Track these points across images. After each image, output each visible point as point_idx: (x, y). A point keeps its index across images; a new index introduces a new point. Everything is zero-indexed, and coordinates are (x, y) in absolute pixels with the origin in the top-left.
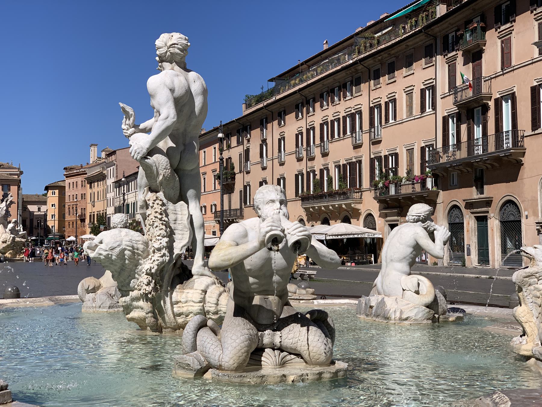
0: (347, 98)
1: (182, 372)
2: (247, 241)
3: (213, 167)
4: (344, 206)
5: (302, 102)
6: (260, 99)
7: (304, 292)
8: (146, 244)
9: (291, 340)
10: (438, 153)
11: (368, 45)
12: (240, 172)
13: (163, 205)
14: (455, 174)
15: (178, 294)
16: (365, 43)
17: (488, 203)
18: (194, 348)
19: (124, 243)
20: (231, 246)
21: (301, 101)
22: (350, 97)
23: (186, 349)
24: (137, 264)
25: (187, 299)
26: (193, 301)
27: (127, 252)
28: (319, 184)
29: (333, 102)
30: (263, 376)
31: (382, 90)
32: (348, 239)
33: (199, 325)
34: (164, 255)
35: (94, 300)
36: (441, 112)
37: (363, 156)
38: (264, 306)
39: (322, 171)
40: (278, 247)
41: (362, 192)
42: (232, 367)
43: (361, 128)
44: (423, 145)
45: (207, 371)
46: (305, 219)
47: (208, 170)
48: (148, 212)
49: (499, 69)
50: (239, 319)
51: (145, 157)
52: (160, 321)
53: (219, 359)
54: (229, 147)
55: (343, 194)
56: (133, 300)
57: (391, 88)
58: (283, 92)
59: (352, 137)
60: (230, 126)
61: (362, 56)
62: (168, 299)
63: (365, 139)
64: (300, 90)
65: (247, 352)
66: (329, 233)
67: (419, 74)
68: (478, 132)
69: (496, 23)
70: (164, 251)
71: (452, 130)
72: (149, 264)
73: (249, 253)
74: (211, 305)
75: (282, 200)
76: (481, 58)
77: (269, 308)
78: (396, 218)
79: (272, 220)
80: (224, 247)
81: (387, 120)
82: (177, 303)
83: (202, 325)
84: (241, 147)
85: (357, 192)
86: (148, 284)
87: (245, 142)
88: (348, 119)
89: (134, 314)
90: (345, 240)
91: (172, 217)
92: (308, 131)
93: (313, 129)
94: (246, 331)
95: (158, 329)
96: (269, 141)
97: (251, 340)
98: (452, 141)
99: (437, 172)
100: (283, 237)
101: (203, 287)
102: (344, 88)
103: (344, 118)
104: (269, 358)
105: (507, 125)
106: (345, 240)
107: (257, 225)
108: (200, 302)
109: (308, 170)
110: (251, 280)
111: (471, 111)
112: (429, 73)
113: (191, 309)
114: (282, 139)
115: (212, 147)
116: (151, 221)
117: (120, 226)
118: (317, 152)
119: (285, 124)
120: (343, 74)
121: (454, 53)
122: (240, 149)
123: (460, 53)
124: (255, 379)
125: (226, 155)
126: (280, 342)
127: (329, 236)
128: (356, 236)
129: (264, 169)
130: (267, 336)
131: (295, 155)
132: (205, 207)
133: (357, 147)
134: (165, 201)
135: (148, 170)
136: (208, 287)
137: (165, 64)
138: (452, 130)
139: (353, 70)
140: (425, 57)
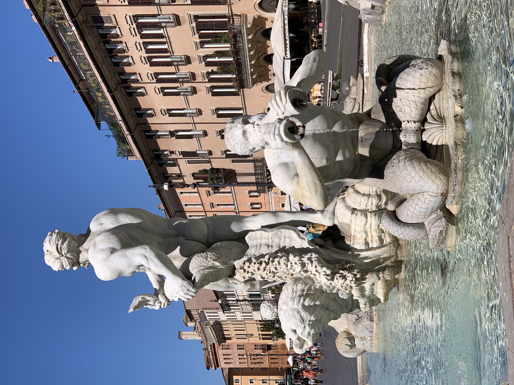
0: (119, 33)
1: (450, 240)
2: (293, 163)
3: (204, 195)
4: (250, 37)
5: (125, 88)
7: (354, 89)
8: (297, 280)
9: (413, 109)
11: (52, 7)
12: (210, 162)
13: (249, 260)
15: (356, 242)
16: (50, 11)
18: (420, 226)
19: (295, 306)
20: (298, 183)
21: (123, 90)
22: (118, 29)
23: (422, 235)
24: (321, 291)
25: (362, 232)
26: (365, 225)
27: (306, 303)
28: (224, 67)
30: (456, 144)
32: (290, 32)
33: (393, 221)
34: (310, 259)
35: (363, 339)
37: (189, 13)
38: (371, 142)
39: (208, 64)
40: (300, 126)
41: (232, 15)
42: (444, 181)
43: (154, 16)
45: (448, 210)
46: (266, 84)
47: (208, 201)
48: (258, 278)
50: (387, 172)
51: (193, 283)
52: (388, 263)
53: (435, 197)
54: (180, 176)
55: (235, 38)
56: (363, 295)
58: (113, 112)
59: (166, 27)
60: (155, 174)
61: (67, 14)
62: (363, 254)
64: (109, 90)
65: (426, 163)
70: (305, 260)
72: (320, 276)
73: (307, 162)
74: (370, 203)
75: (242, 121)
77: (373, 136)
79: (267, 134)
80: (300, 191)
82: (367, 243)
83: (394, 216)
84: (179, 161)
85: (233, 21)
86: (344, 277)
87: (173, 156)
88: (144, 32)
89: (380, 293)
90: (291, 35)
91: (264, 250)
92: (159, 81)
93: (156, 74)
94: (401, 164)
95: (397, 266)
96: (173, 128)
97: (411, 158)
100: (288, 120)
101: (349, 213)
102: (106, 38)
103: (143, 36)
104: (434, 136)
106: (291, 35)
107: (274, 151)
108: (366, 216)
109: (207, 80)
110: (339, 158)
113: (374, 227)
114: (170, 112)
115: (180, 196)
116: (269, 275)
117: (275, 310)
118: (185, 70)
119: (151, 109)
120: (88, 38)
122: (183, 162)
124: (459, 154)
125: (189, 180)
126: (414, 122)
127: (286, 54)
128: (286, 22)
129: (205, 134)
130: (407, 138)
131: (189, 97)
132: (252, 204)
133: (177, 21)
134: (245, 258)
135: (206, 279)
136: (348, 207)
137: (82, 259)
139: (84, 26)
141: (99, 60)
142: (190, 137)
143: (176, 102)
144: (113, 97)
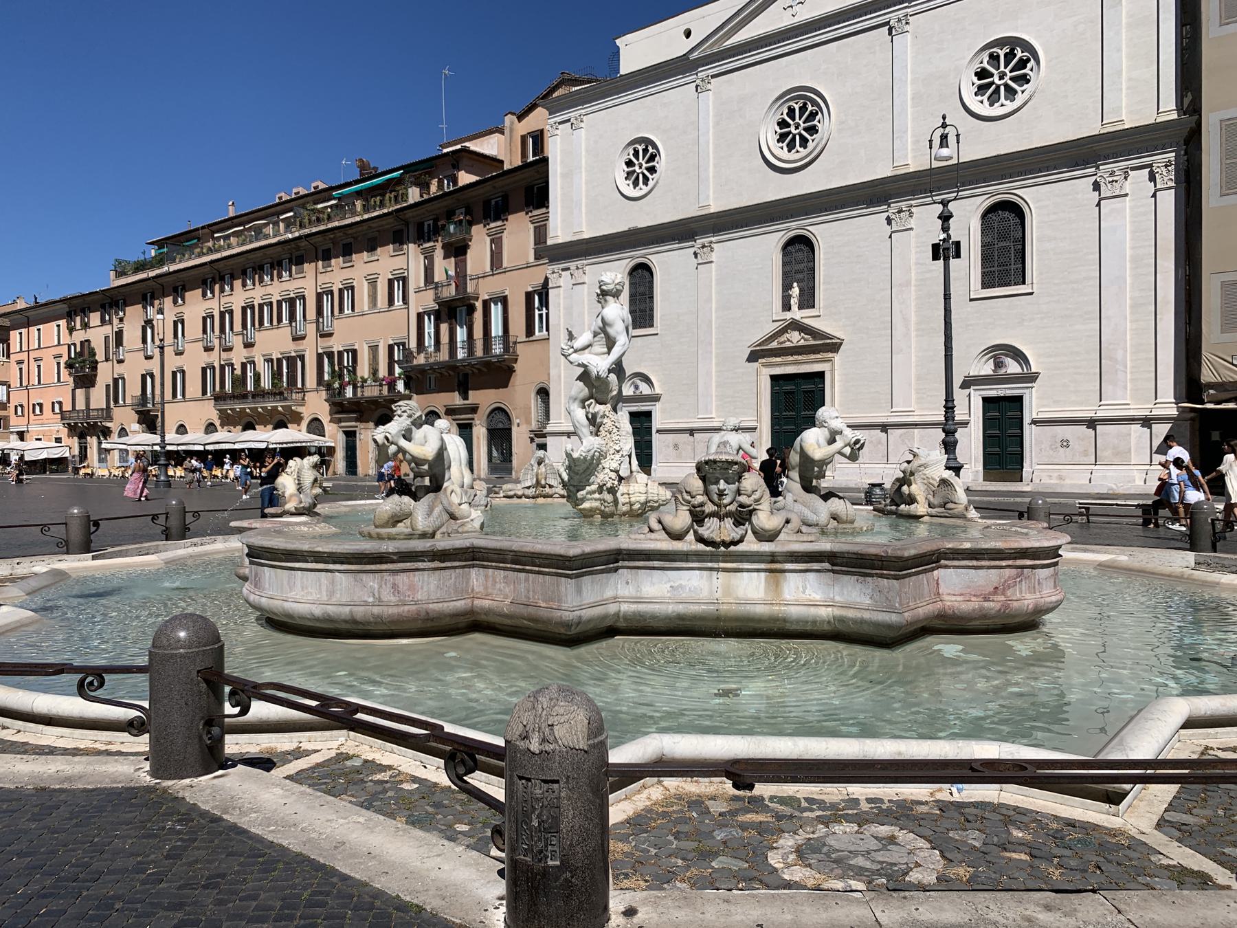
5: (214, 277)
6: (140, 267)
10: (412, 353)
11: (314, 218)
12: (107, 360)
14: (433, 377)
17: (474, 409)
28: (240, 381)
29: (261, 280)
31: (336, 274)
36: (414, 309)
39: (244, 366)
44: (391, 342)
46: (217, 423)
47: (48, 355)
49: (488, 269)
54: (86, 326)
55: (277, 393)
57: (347, 274)
58: (180, 261)
63: (311, 329)
64: (212, 262)
66: (273, 440)
67: (385, 262)
68: (461, 334)
69: (485, 218)
71: (429, 328)
76: (465, 253)
78: (353, 424)
81: (341, 310)
87: (115, 321)
92: (222, 314)
93: (231, 312)
98: (429, 341)
99: (412, 374)
103: (279, 303)
105: (496, 329)
111: (453, 310)
112: (399, 262)
114: (179, 321)
115: (54, 324)
120: (279, 249)
121: (431, 244)
123: (439, 245)
125: (79, 336)
129: (148, 358)
132: (41, 405)
133: (297, 338)
137: (609, 298)
138: (429, 328)
140: (393, 243)
141: (251, 256)
142: (144, 341)
143: (193, 328)
144: (205, 264)
